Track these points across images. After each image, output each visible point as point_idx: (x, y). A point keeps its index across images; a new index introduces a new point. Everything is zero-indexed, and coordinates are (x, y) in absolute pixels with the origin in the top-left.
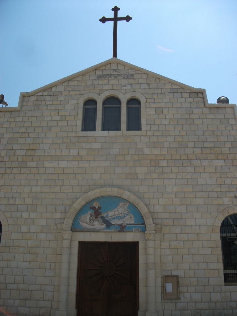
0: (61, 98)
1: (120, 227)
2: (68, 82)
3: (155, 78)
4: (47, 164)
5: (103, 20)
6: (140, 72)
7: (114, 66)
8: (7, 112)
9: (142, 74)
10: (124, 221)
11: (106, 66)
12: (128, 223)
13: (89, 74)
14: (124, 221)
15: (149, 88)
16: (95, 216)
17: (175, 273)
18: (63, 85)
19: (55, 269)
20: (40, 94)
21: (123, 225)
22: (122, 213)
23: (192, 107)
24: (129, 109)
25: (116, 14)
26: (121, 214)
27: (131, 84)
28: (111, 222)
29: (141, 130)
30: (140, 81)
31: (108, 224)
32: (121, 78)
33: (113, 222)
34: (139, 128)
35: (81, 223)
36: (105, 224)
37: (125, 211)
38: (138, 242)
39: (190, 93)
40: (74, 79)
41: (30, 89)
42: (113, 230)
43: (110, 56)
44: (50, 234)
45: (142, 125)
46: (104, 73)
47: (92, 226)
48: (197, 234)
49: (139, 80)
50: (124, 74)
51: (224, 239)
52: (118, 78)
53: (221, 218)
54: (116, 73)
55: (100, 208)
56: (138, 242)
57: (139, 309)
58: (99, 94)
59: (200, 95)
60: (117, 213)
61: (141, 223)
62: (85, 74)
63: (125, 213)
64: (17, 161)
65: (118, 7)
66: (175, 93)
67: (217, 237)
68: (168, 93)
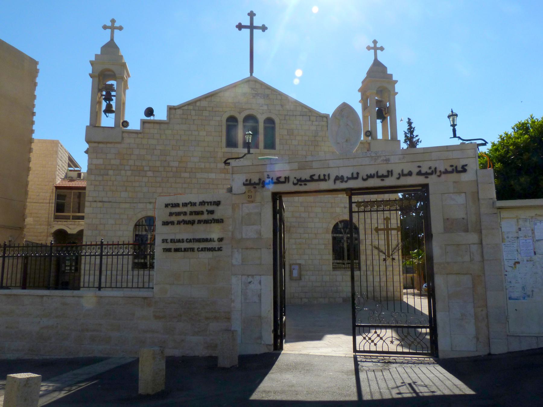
0: (206, 113)
4: (199, 175)
5: (240, 27)
6: (275, 93)
17: (299, 262)
20: (186, 108)
24: (265, 128)
27: (267, 105)
29: (275, 149)
32: (259, 97)
39: (317, 117)
41: (176, 103)
43: (248, 75)
48: (315, 234)
50: (262, 94)
51: (334, 238)
53: (334, 223)
58: (240, 113)
59: (325, 119)
64: (172, 172)
65: (254, 12)
67: (329, 237)
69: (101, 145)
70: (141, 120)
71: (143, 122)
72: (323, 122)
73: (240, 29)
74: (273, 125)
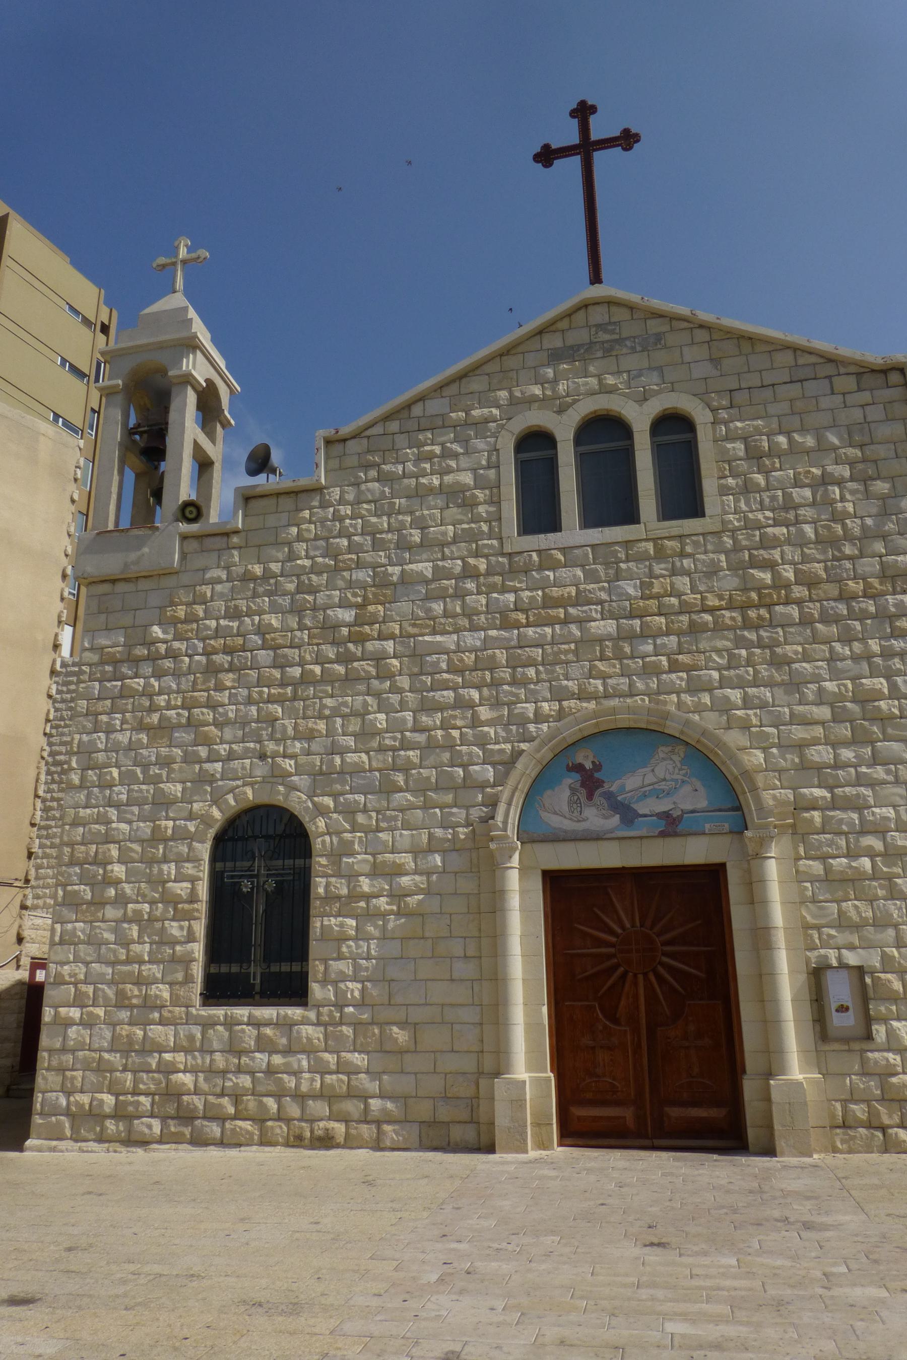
1: (663, 822)
2: (457, 384)
3: (738, 338)
6: (685, 325)
7: (598, 315)
8: (283, 496)
9: (691, 328)
10: (674, 803)
11: (573, 317)
12: (689, 807)
13: (520, 349)
14: (674, 803)
15: (718, 373)
16: (583, 791)
18: (444, 394)
19: (480, 957)
20: (378, 430)
21: (674, 816)
22: (668, 777)
23: (869, 423)
24: (658, 450)
25: (584, 129)
26: (664, 783)
28: (635, 806)
29: (703, 515)
30: (689, 354)
31: (628, 815)
32: (625, 351)
33: (642, 808)
34: (695, 509)
35: (545, 815)
36: (618, 816)
37: (677, 771)
38: (723, 866)
39: (859, 375)
40: (477, 372)
42: (643, 832)
44: (454, 853)
45: (706, 499)
46: (569, 343)
47: (579, 821)
49: (686, 350)
50: (634, 337)
52: (614, 353)
54: (607, 337)
55: (597, 767)
56: (723, 866)
57: (744, 1071)
60: (650, 779)
61: (729, 806)
62: (508, 351)
63: (675, 777)
66: (806, 380)
68: (785, 383)
69: (121, 587)
70: (237, 490)
71: (243, 495)
72: (888, 387)
73: (547, 163)
74: (687, 436)
